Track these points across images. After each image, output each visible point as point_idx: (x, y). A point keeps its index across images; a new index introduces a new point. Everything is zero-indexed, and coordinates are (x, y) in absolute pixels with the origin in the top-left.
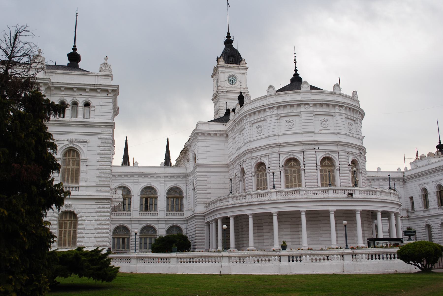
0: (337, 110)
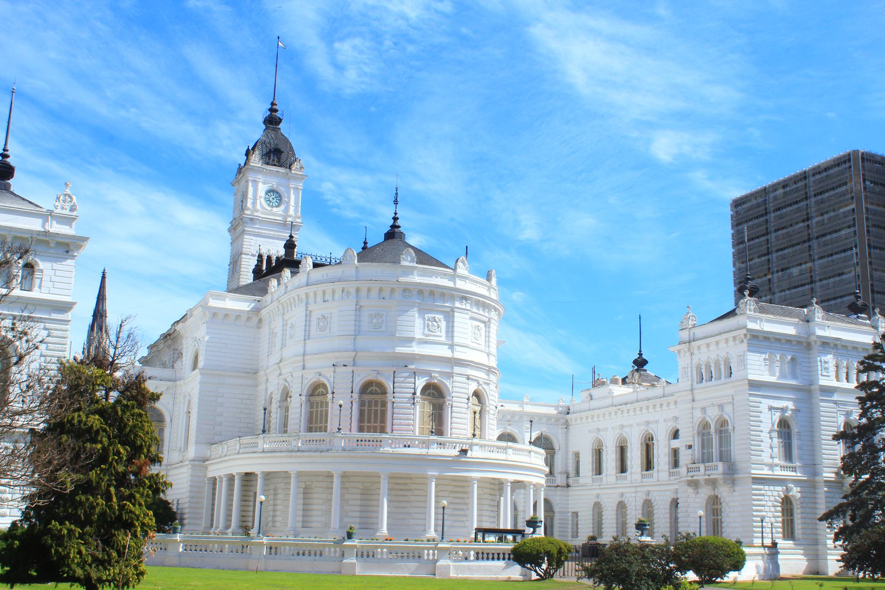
0: (457, 304)
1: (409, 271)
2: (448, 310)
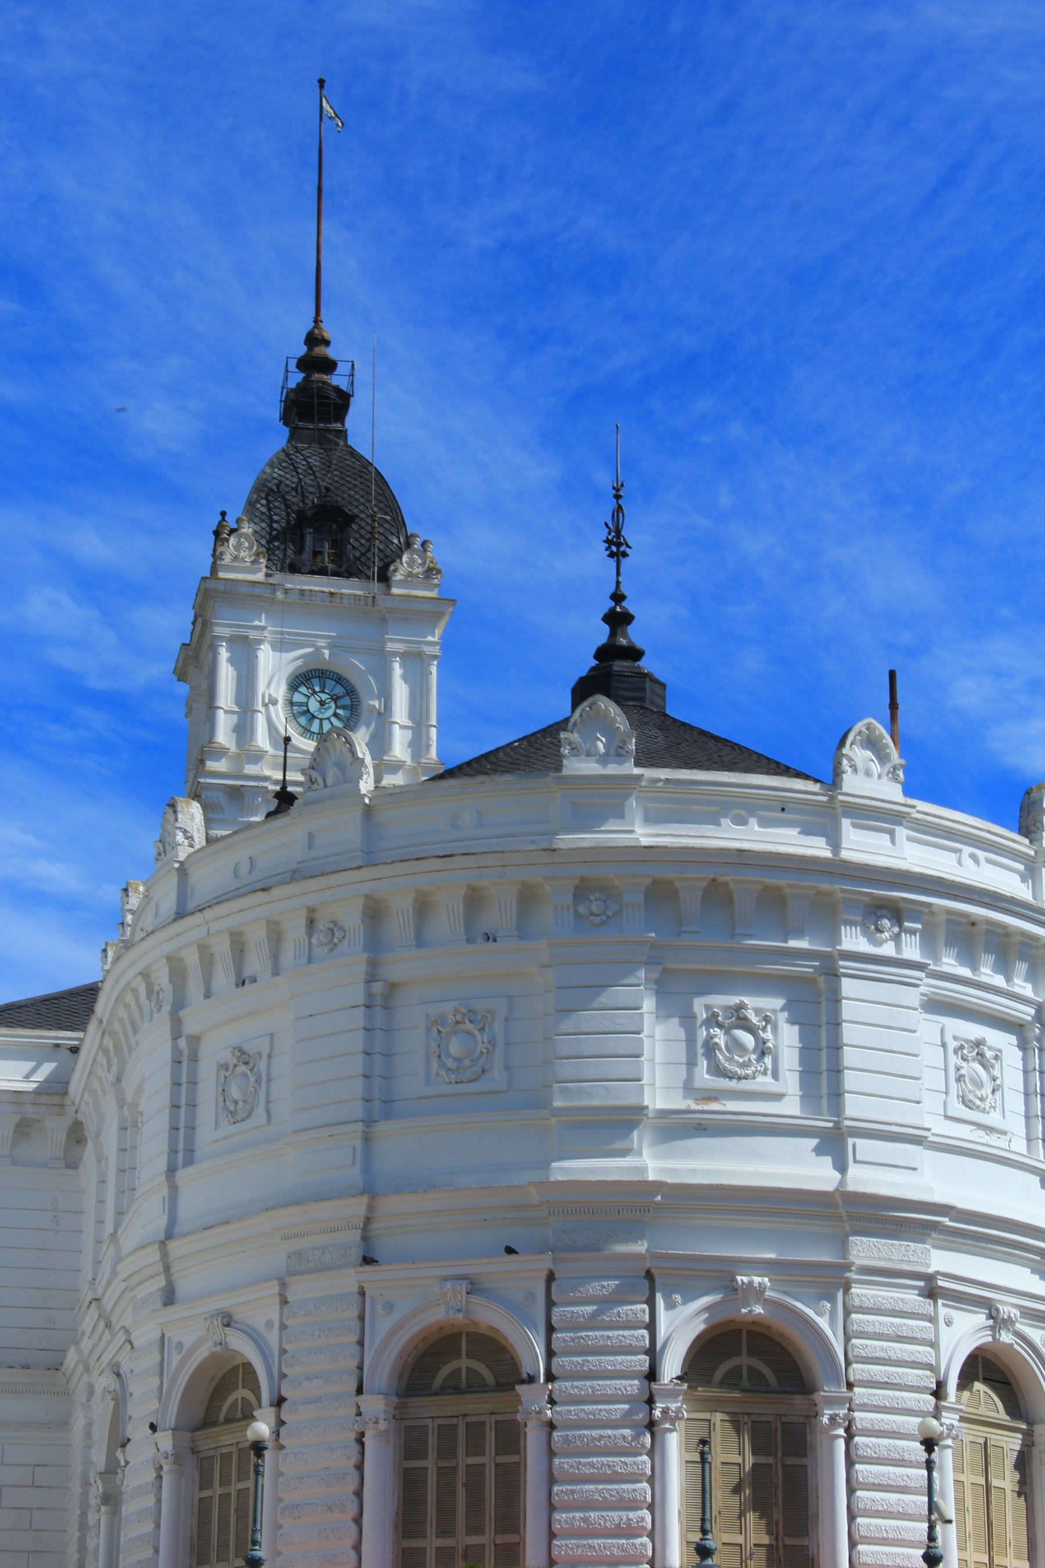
0: (853, 940)
1: (606, 799)
2: (806, 968)
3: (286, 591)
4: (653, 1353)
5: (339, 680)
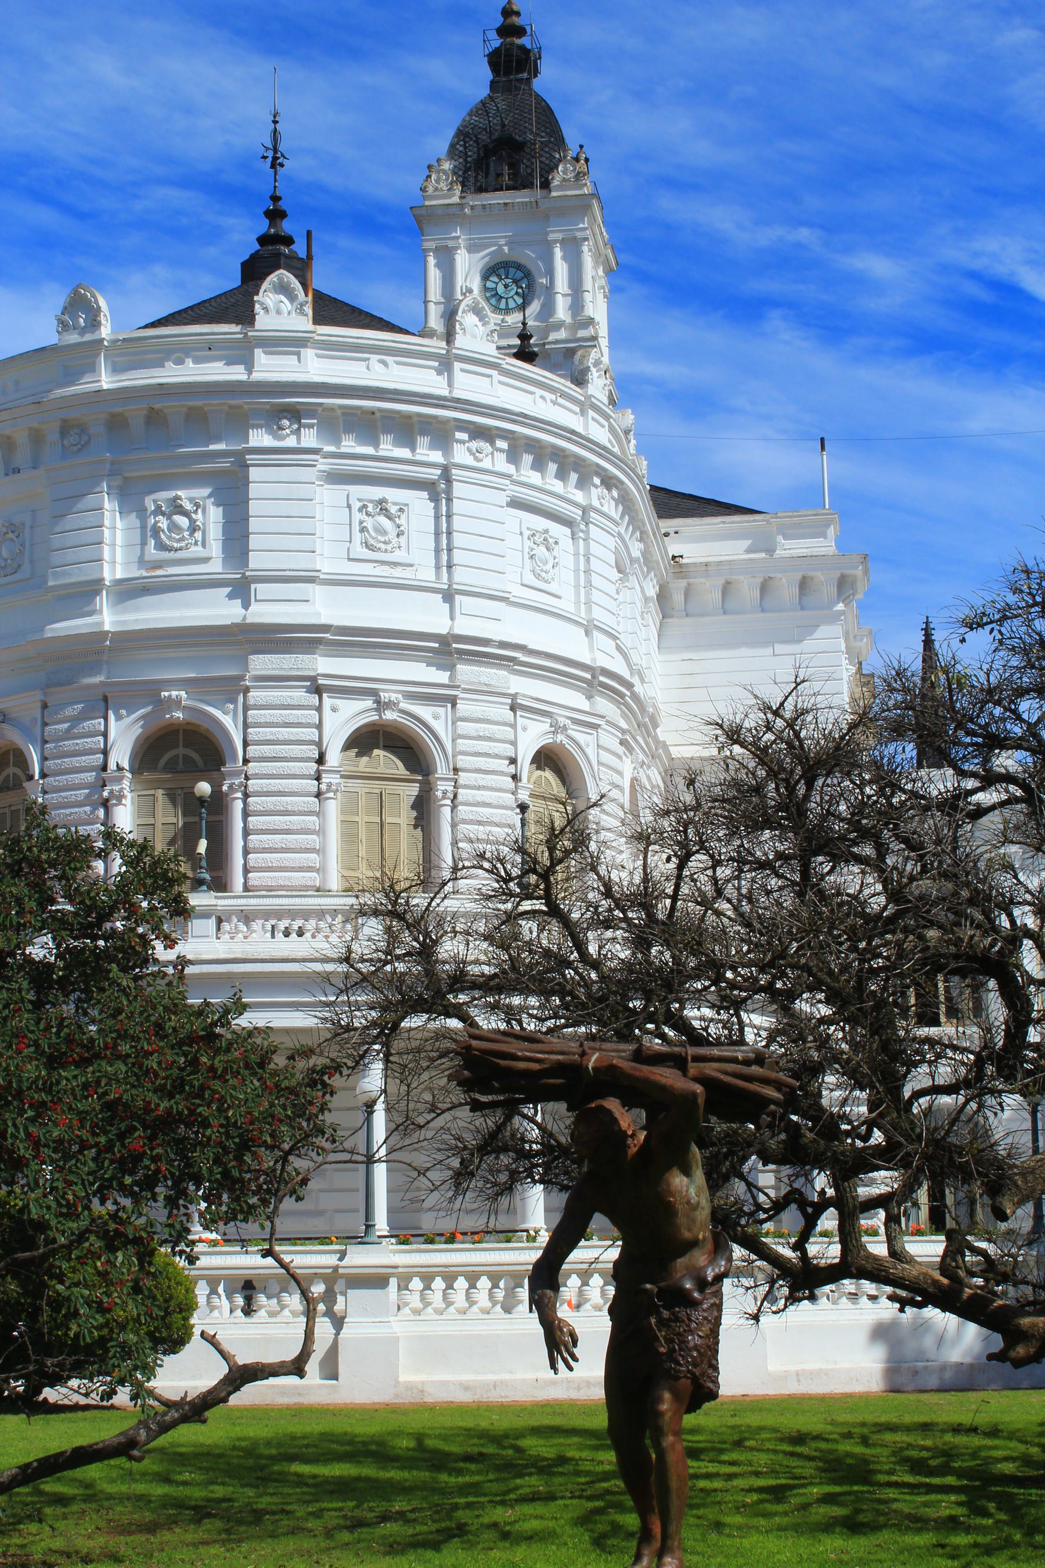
0: (258, 438)
2: (225, 464)
3: (472, 208)
4: (105, 752)
5: (519, 267)
